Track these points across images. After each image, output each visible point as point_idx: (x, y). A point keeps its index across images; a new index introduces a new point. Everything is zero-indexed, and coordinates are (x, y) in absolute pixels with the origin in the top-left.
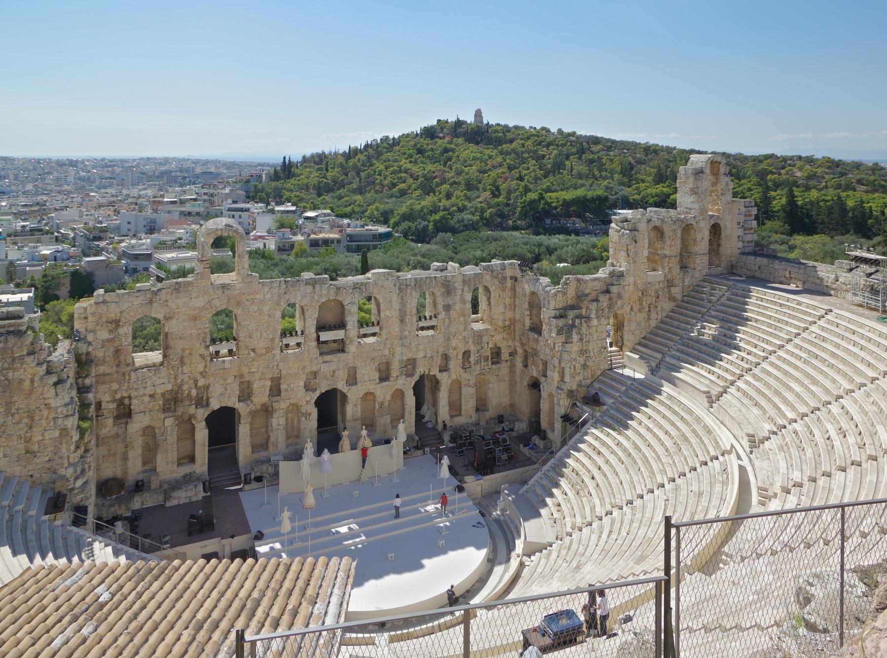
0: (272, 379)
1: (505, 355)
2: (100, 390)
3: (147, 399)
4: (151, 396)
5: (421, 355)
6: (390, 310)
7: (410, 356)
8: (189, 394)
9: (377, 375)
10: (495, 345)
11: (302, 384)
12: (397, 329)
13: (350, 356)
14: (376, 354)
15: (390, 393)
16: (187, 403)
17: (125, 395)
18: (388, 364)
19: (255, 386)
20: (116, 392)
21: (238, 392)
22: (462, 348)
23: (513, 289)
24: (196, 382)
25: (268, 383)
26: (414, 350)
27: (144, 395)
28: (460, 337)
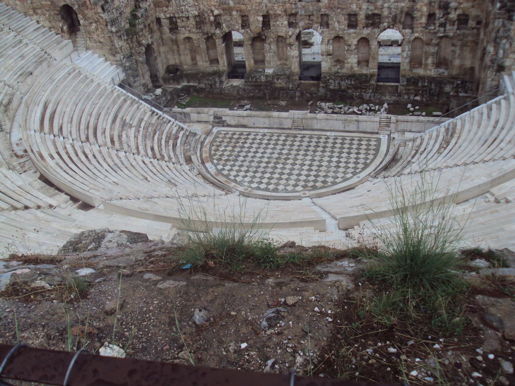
0: (264, 17)
2: (158, 11)
3: (185, 19)
4: (188, 18)
7: (376, 12)
8: (209, 19)
9: (346, 23)
11: (286, 23)
15: (357, 39)
16: (209, 25)
17: (172, 15)
18: (355, 15)
19: (251, 19)
20: (165, 12)
21: (240, 22)
24: (212, 12)
25: (261, 19)
27: (182, 17)
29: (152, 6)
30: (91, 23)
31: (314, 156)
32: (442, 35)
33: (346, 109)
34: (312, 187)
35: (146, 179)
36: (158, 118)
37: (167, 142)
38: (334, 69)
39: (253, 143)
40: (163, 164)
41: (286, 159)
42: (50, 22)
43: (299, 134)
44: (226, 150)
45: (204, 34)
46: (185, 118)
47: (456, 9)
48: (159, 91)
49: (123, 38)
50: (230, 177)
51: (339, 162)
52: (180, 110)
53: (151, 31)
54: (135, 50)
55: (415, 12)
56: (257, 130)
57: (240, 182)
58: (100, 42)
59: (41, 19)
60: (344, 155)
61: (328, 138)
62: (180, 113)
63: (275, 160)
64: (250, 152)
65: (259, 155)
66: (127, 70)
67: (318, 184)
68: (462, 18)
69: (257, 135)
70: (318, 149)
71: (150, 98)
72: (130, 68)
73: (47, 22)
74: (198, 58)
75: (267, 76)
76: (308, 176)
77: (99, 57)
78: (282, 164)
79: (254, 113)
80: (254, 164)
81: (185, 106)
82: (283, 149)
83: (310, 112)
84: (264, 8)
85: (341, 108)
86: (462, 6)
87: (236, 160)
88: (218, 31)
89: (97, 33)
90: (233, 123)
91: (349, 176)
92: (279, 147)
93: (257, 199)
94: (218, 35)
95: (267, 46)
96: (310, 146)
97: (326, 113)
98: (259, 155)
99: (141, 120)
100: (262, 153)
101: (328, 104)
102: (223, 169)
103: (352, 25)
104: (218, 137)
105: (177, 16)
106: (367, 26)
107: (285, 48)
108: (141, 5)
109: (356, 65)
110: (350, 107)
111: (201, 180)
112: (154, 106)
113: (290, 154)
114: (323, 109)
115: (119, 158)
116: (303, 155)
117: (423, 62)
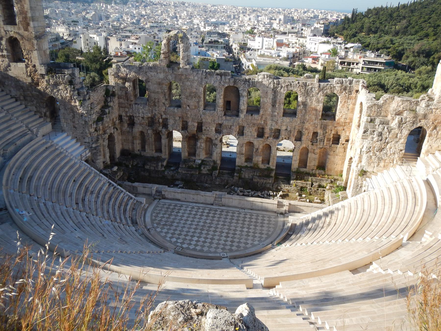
0: (198, 122)
1: (342, 140)
3: (141, 119)
4: (143, 118)
5: (284, 128)
6: (267, 98)
7: (277, 127)
8: (159, 120)
9: (256, 134)
10: (337, 132)
11: (214, 129)
12: (270, 110)
13: (240, 119)
14: (255, 122)
16: (158, 125)
17: (131, 115)
18: (263, 129)
19: (190, 124)
21: (181, 125)
22: (312, 130)
23: (356, 98)
24: (161, 116)
25: (196, 124)
26: (279, 124)
27: (139, 117)
28: (312, 123)
29: (117, 106)
30: (70, 112)
31: (230, 226)
32: (321, 147)
33: (253, 193)
34: (229, 250)
35: (103, 235)
36: (114, 188)
37: (119, 207)
38: (246, 164)
39: (185, 213)
40: (116, 224)
41: (210, 227)
42: (36, 107)
43: (219, 209)
44: (164, 217)
45: (153, 130)
46: (133, 190)
47: (331, 130)
48: (115, 169)
49: (93, 126)
50: (166, 238)
51: (248, 232)
52: (130, 184)
53: (114, 124)
54: (102, 137)
55: (304, 130)
56: (188, 204)
57: (174, 242)
58: (74, 127)
59: (29, 104)
60: (252, 227)
61: (240, 213)
62: (130, 186)
63: (201, 227)
64: (182, 220)
65: (189, 222)
66: (93, 150)
67: (234, 248)
68: (336, 136)
69: (188, 207)
70: (233, 221)
71: (108, 173)
72: (95, 148)
73: (34, 107)
74: (146, 147)
75: (196, 165)
76: (226, 241)
77: (72, 139)
78: (206, 230)
79: (186, 190)
80: (185, 230)
81: (133, 182)
82: (207, 219)
83: (227, 194)
84: (199, 117)
85: (249, 192)
86: (336, 129)
87: (171, 225)
88: (164, 130)
89: (73, 120)
90: (170, 196)
91: (256, 243)
92: (204, 218)
93: (188, 258)
94: (163, 132)
95: (199, 144)
96: (227, 218)
97: (238, 195)
98: (189, 222)
99: (101, 189)
100: (191, 221)
101: (240, 188)
102: (161, 232)
103: (261, 134)
104: (158, 207)
105: (135, 115)
106: (270, 136)
107: (211, 147)
108: (109, 104)
109: (261, 163)
110: (255, 192)
111: (144, 240)
112: (110, 178)
113: (212, 223)
114: (236, 192)
115: (82, 217)
116: (222, 225)
117: (308, 164)
